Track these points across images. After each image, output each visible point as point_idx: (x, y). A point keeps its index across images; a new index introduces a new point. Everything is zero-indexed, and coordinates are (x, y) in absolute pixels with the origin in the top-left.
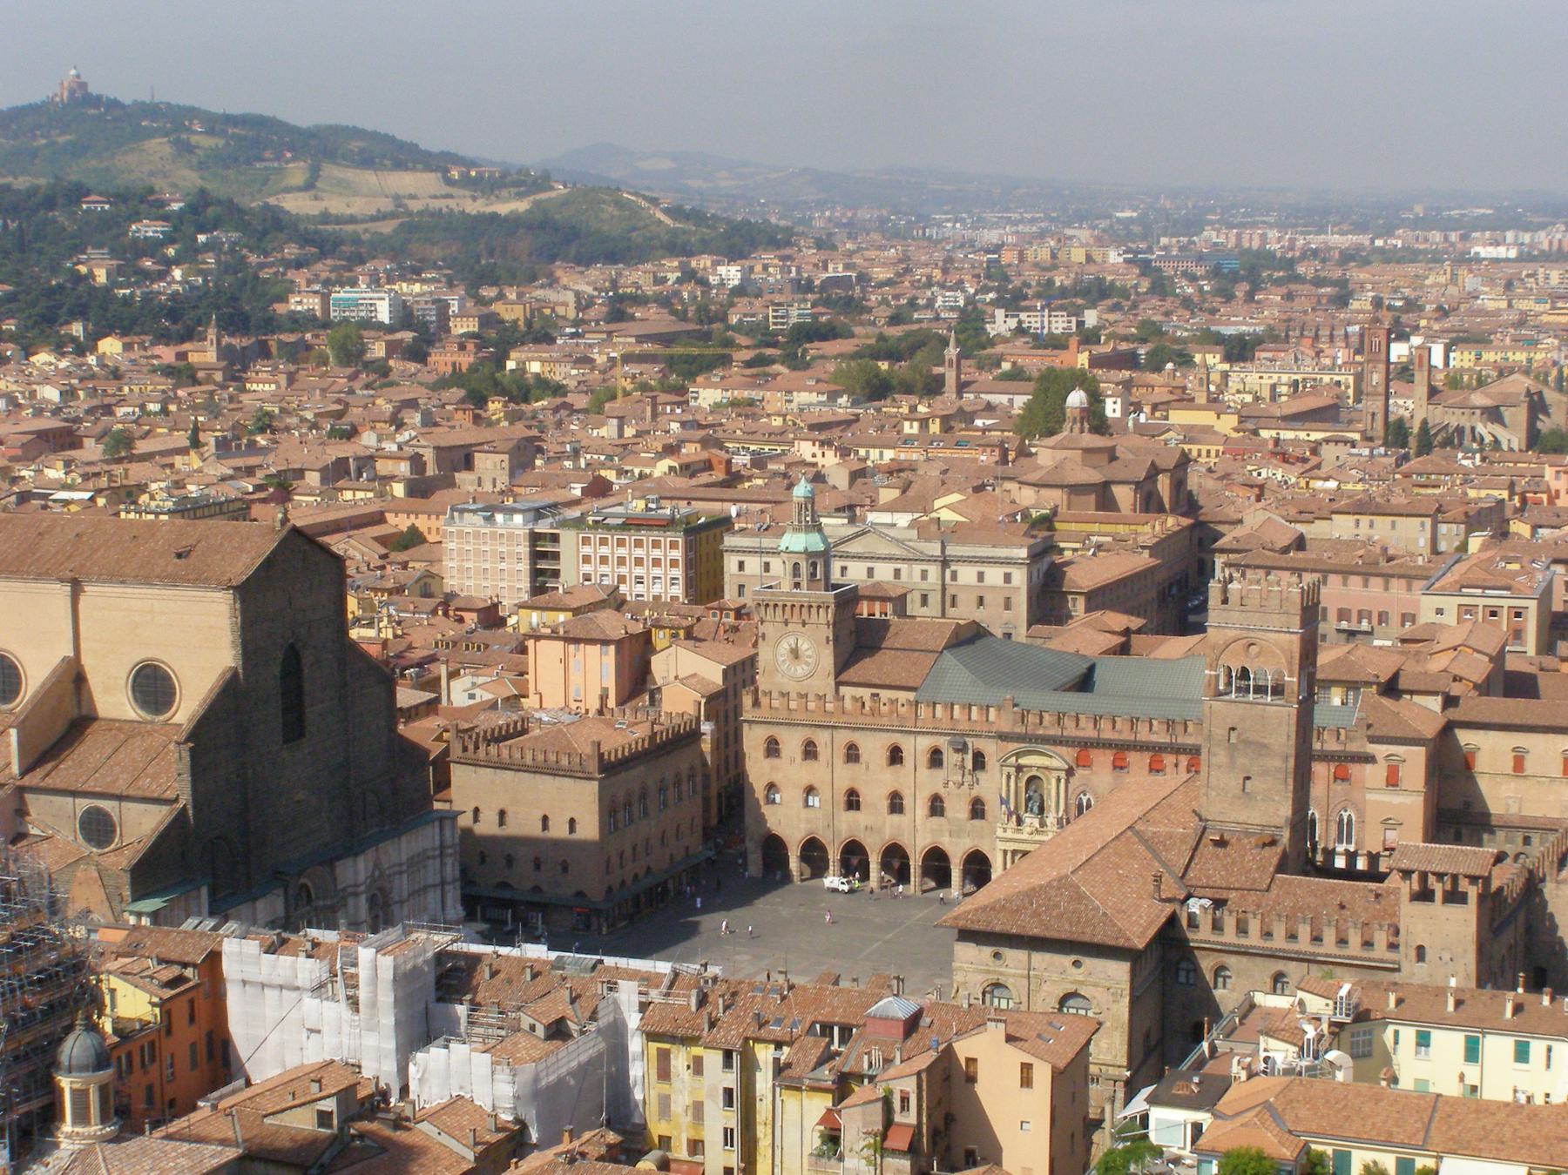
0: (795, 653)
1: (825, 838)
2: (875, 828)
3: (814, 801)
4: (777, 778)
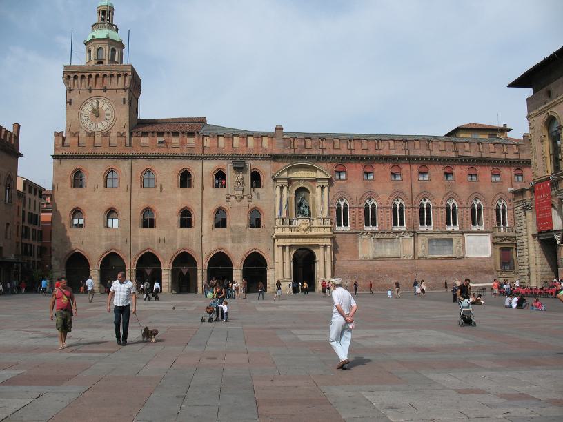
0: (97, 113)
1: (123, 251)
2: (166, 240)
3: (114, 223)
4: (82, 204)
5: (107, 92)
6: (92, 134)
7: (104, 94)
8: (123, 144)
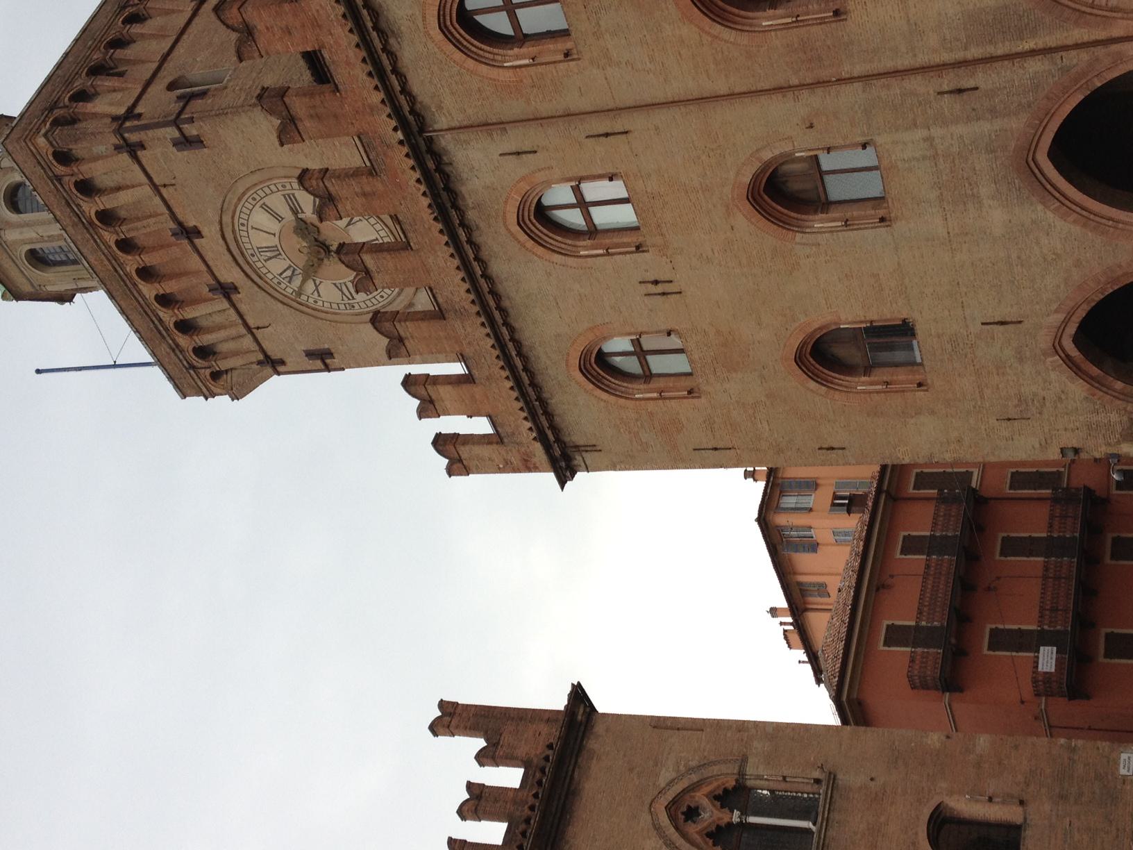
5: (191, 222)
7: (210, 232)
8: (367, 184)
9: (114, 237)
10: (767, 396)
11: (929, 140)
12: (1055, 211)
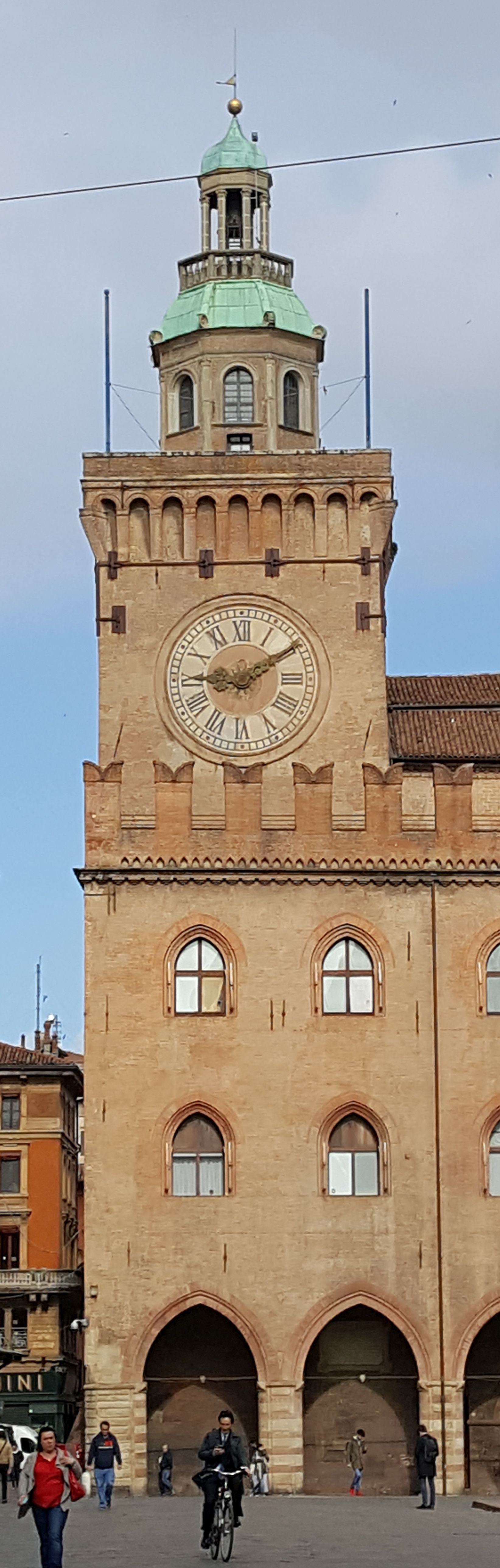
6: (245, 775)
7: (271, 586)
9: (284, 500)
10: (163, 1071)
11: (387, 1232)
12: (319, 1304)
